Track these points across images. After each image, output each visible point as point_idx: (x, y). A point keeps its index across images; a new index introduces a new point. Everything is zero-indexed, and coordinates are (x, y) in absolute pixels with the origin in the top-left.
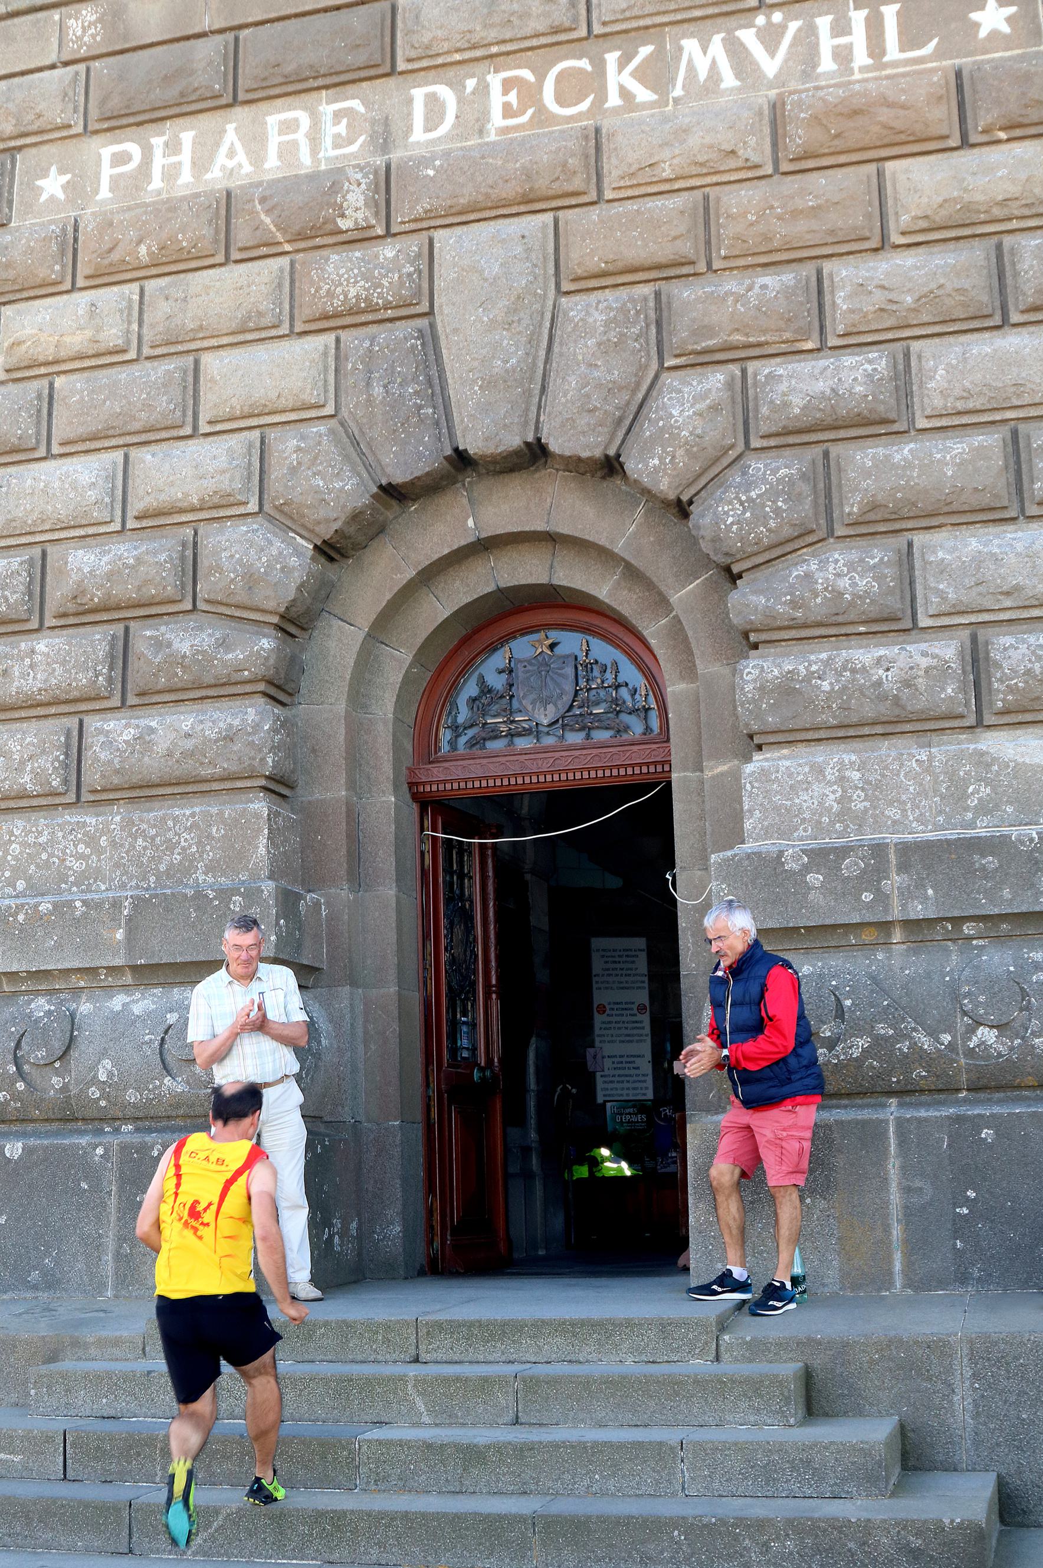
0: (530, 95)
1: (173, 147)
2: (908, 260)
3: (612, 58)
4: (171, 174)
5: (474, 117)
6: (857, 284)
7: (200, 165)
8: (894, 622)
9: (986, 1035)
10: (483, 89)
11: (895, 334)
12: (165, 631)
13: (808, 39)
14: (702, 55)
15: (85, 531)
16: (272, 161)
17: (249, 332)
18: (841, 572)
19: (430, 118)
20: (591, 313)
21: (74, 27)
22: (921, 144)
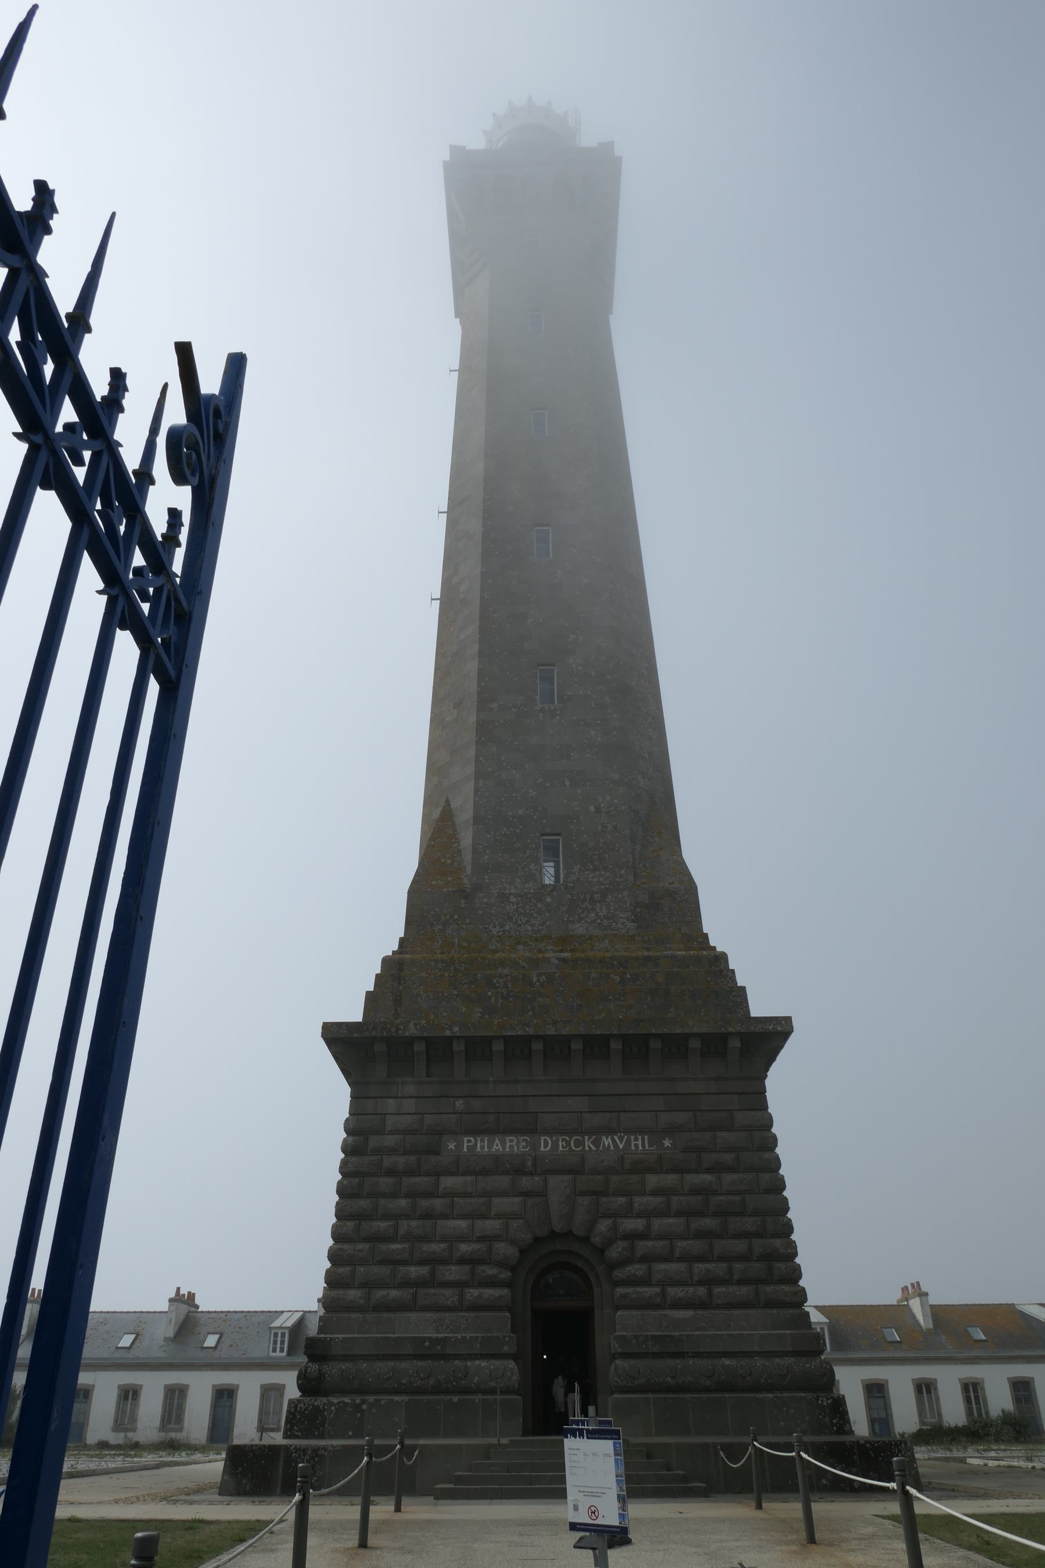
0: (568, 1144)
1: (482, 1141)
2: (650, 1198)
3: (586, 1137)
4: (482, 1147)
5: (555, 1145)
6: (639, 1202)
7: (490, 1147)
8: (646, 1282)
9: (669, 1379)
10: (557, 1140)
11: (647, 1214)
12: (485, 1268)
13: (628, 1142)
14: (607, 1141)
15: (463, 1239)
16: (507, 1149)
17: (503, 1194)
18: (637, 1269)
19: (545, 1144)
20: (584, 1201)
21: (457, 1104)
22: (653, 1171)
